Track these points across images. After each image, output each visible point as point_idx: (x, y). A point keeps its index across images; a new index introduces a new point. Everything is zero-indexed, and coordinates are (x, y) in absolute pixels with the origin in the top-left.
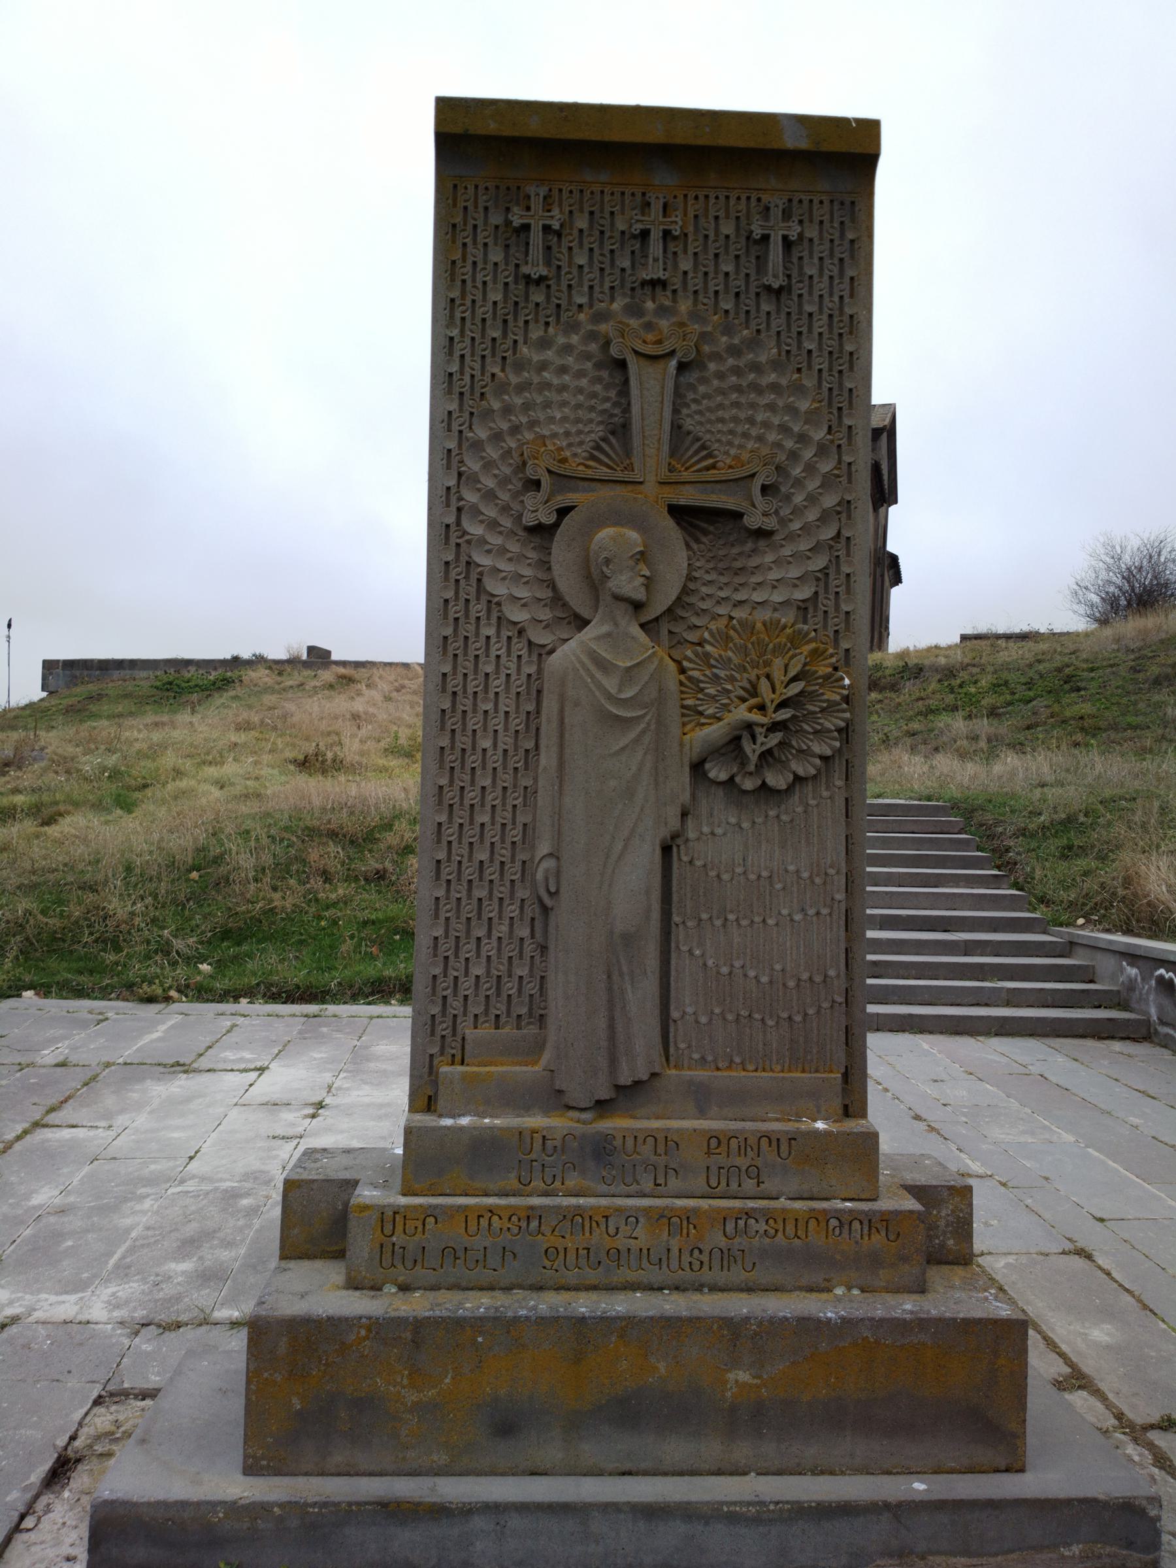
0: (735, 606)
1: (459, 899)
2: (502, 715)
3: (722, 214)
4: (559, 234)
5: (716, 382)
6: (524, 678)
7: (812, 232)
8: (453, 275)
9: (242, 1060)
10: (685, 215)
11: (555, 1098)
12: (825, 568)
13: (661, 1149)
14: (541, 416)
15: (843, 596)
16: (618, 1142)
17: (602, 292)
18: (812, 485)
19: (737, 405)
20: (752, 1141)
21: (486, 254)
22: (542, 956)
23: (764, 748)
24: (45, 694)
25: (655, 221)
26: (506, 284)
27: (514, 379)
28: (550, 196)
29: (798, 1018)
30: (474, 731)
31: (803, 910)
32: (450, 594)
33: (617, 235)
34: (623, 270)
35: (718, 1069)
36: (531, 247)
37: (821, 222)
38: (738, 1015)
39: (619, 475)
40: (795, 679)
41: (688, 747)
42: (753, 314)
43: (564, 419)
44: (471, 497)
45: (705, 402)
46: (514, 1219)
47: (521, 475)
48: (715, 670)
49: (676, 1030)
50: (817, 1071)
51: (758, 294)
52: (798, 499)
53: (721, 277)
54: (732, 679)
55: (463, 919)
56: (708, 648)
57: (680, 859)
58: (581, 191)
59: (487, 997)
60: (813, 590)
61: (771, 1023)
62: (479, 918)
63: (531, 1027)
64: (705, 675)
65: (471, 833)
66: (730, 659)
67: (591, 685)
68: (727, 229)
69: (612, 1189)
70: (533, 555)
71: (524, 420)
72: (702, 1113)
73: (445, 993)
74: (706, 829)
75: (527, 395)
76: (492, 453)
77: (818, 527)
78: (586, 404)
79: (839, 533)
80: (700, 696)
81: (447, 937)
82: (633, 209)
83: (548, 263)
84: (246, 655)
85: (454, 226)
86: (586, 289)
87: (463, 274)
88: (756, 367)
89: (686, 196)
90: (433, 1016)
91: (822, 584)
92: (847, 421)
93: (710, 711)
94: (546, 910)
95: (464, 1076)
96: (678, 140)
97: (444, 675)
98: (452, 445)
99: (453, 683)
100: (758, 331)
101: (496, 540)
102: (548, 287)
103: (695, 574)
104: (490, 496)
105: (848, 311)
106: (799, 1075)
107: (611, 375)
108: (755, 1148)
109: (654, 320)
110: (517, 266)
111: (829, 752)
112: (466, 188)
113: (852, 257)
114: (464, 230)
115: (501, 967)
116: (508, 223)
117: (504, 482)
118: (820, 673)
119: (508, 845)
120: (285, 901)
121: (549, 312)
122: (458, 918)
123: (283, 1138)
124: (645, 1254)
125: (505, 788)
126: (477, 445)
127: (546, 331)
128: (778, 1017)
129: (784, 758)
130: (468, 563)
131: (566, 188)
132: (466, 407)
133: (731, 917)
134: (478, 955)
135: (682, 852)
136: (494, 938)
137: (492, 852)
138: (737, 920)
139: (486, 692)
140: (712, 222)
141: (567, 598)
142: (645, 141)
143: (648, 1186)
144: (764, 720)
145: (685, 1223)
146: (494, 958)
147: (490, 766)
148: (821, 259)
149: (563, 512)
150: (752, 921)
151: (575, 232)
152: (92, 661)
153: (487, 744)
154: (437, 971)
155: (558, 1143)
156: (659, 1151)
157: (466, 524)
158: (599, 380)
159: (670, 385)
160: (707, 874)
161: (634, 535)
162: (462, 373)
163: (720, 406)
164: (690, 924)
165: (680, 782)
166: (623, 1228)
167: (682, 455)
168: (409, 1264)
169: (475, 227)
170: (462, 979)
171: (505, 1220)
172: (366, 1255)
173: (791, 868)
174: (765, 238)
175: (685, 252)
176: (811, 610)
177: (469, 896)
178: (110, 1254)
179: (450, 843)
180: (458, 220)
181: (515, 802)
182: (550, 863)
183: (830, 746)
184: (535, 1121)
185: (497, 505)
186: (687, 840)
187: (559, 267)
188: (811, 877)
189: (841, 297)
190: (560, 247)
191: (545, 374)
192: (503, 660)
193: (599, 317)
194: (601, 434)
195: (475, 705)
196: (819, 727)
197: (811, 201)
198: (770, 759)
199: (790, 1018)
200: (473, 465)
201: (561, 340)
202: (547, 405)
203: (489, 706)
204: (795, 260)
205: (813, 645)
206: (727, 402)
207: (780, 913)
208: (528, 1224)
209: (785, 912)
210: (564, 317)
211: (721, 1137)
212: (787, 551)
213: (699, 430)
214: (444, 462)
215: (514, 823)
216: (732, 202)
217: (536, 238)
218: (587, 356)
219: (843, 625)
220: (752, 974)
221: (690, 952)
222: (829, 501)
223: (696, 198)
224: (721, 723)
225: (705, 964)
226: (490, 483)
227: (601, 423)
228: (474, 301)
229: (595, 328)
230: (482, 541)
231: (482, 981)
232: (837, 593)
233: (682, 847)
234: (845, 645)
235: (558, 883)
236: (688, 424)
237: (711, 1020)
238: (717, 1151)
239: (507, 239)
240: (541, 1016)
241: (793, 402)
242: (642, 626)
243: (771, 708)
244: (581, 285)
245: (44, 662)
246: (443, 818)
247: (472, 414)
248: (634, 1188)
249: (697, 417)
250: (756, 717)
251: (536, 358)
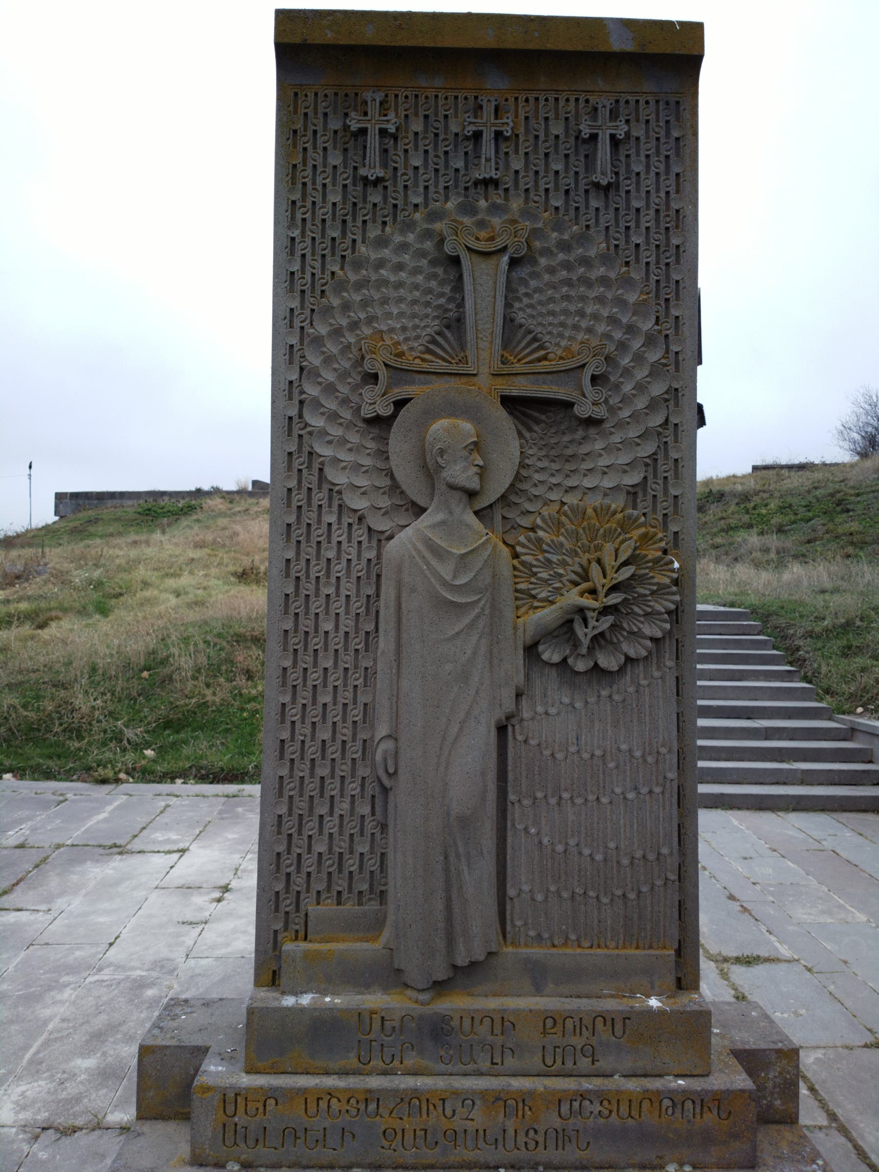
0: (566, 491)
1: (302, 778)
2: (343, 599)
3: (551, 115)
4: (395, 138)
5: (547, 277)
6: (364, 562)
7: (638, 131)
8: (293, 178)
9: (168, 841)
10: (516, 117)
11: (391, 976)
13: (498, 1030)
14: (379, 312)
15: (671, 481)
16: (455, 1023)
17: (436, 192)
18: (641, 374)
19: (567, 298)
20: (587, 1021)
21: (325, 158)
22: (382, 833)
23: (596, 632)
24: (57, 518)
25: (487, 123)
26: (345, 186)
27: (353, 277)
28: (387, 102)
29: (632, 896)
30: (317, 614)
31: (636, 788)
32: (292, 484)
33: (451, 138)
34: (457, 170)
35: (554, 946)
36: (368, 150)
37: (647, 121)
38: (573, 893)
39: (454, 368)
40: (625, 564)
41: (522, 629)
42: (582, 210)
43: (401, 314)
44: (312, 391)
45: (536, 296)
46: (353, 1101)
47: (360, 369)
48: (547, 555)
49: (513, 908)
50: (651, 947)
51: (587, 191)
52: (627, 388)
53: (551, 175)
54: (564, 564)
55: (306, 797)
56: (541, 533)
57: (515, 738)
58: (416, 96)
59: (330, 873)
60: (642, 475)
61: (605, 900)
62: (322, 796)
63: (373, 903)
64: (537, 560)
65: (313, 713)
66: (562, 545)
67: (428, 573)
68: (557, 129)
69: (450, 1068)
70: (371, 445)
71: (362, 316)
72: (538, 990)
73: (288, 870)
74: (540, 709)
75: (366, 292)
76: (332, 348)
77: (647, 414)
78: (422, 300)
79: (667, 421)
80: (533, 580)
81: (290, 815)
82: (467, 112)
83: (384, 165)
84: (206, 487)
85: (295, 132)
86: (421, 189)
87: (304, 178)
88: (585, 261)
89: (516, 99)
90: (277, 893)
91: (651, 469)
92: (674, 312)
93: (543, 595)
94: (385, 790)
95: (306, 954)
96: (509, 45)
97: (288, 561)
98: (294, 340)
99: (298, 568)
100: (588, 227)
101: (336, 431)
102: (385, 188)
103: (527, 461)
104: (330, 389)
105: (674, 206)
106: (632, 952)
107: (445, 271)
108: (590, 1027)
109: (487, 218)
110: (355, 168)
111: (659, 634)
112: (306, 96)
113: (678, 154)
114: (305, 135)
115: (342, 844)
116: (346, 128)
117: (343, 375)
118: (650, 557)
119: (349, 724)
120: (214, 697)
121: (386, 212)
122: (301, 796)
123: (191, 923)
124: (480, 1135)
125: (346, 669)
126: (318, 341)
127: (383, 231)
128: (613, 894)
129: (615, 640)
130: (310, 453)
131: (402, 93)
132: (307, 304)
133: (566, 795)
134: (321, 833)
135: (517, 734)
136: (336, 815)
137: (334, 732)
138: (571, 798)
139: (328, 577)
140: (543, 123)
141: (404, 487)
142: (477, 46)
143: (484, 1064)
145: (520, 1105)
146: (336, 835)
147: (332, 647)
148: (647, 156)
149: (400, 404)
150: (586, 800)
151: (411, 136)
152: (91, 493)
153: (328, 626)
154: (281, 848)
155: (397, 1024)
156: (495, 1032)
157: (307, 417)
158: (435, 276)
159: (502, 279)
160: (541, 753)
161: (467, 426)
162: (303, 272)
163: (551, 300)
164: (526, 802)
166: (459, 1110)
167: (515, 347)
169: (315, 132)
170: (305, 856)
171: (344, 1102)
172: (210, 1134)
173: (624, 747)
174: (594, 137)
175: (517, 152)
176: (640, 495)
177: (312, 775)
178: (26, 1048)
179: (293, 723)
180: (299, 126)
181: (356, 683)
182: (388, 745)
183: (660, 628)
184: (374, 1000)
185: (337, 397)
186: (522, 720)
187: (395, 169)
188: (643, 756)
189: (668, 193)
190: (396, 149)
191: (383, 272)
192: (345, 545)
193: (434, 216)
194: (436, 328)
195: (317, 589)
196: (649, 610)
197: (637, 101)
198: (602, 642)
199: (624, 895)
200: (314, 360)
201: (398, 239)
202: (385, 301)
203: (331, 590)
204: (623, 158)
205: (643, 530)
206: (557, 296)
207: (613, 792)
208: (366, 1106)
209: (618, 790)
211: (556, 1018)
212: (617, 438)
213: (531, 323)
214: (287, 357)
215: (355, 703)
216: (562, 103)
217: (373, 141)
218: (423, 254)
219: (671, 509)
220: (586, 852)
221: (526, 829)
222: (658, 389)
223: (527, 100)
224: (553, 607)
225: (540, 843)
226: (329, 376)
227: (437, 317)
228: (314, 203)
229: (430, 227)
230: (323, 433)
231: (325, 858)
232: (666, 478)
233: (517, 727)
234: (673, 528)
235: (396, 764)
236: (520, 317)
237: (546, 897)
238: (553, 1031)
239: (345, 143)
240: (382, 892)
241: (622, 294)
242: (476, 513)
243: (602, 592)
244: (416, 185)
245: (57, 494)
246: (287, 699)
247: (313, 311)
248: (471, 1067)
249: (529, 311)
250: (587, 601)
251: (373, 256)
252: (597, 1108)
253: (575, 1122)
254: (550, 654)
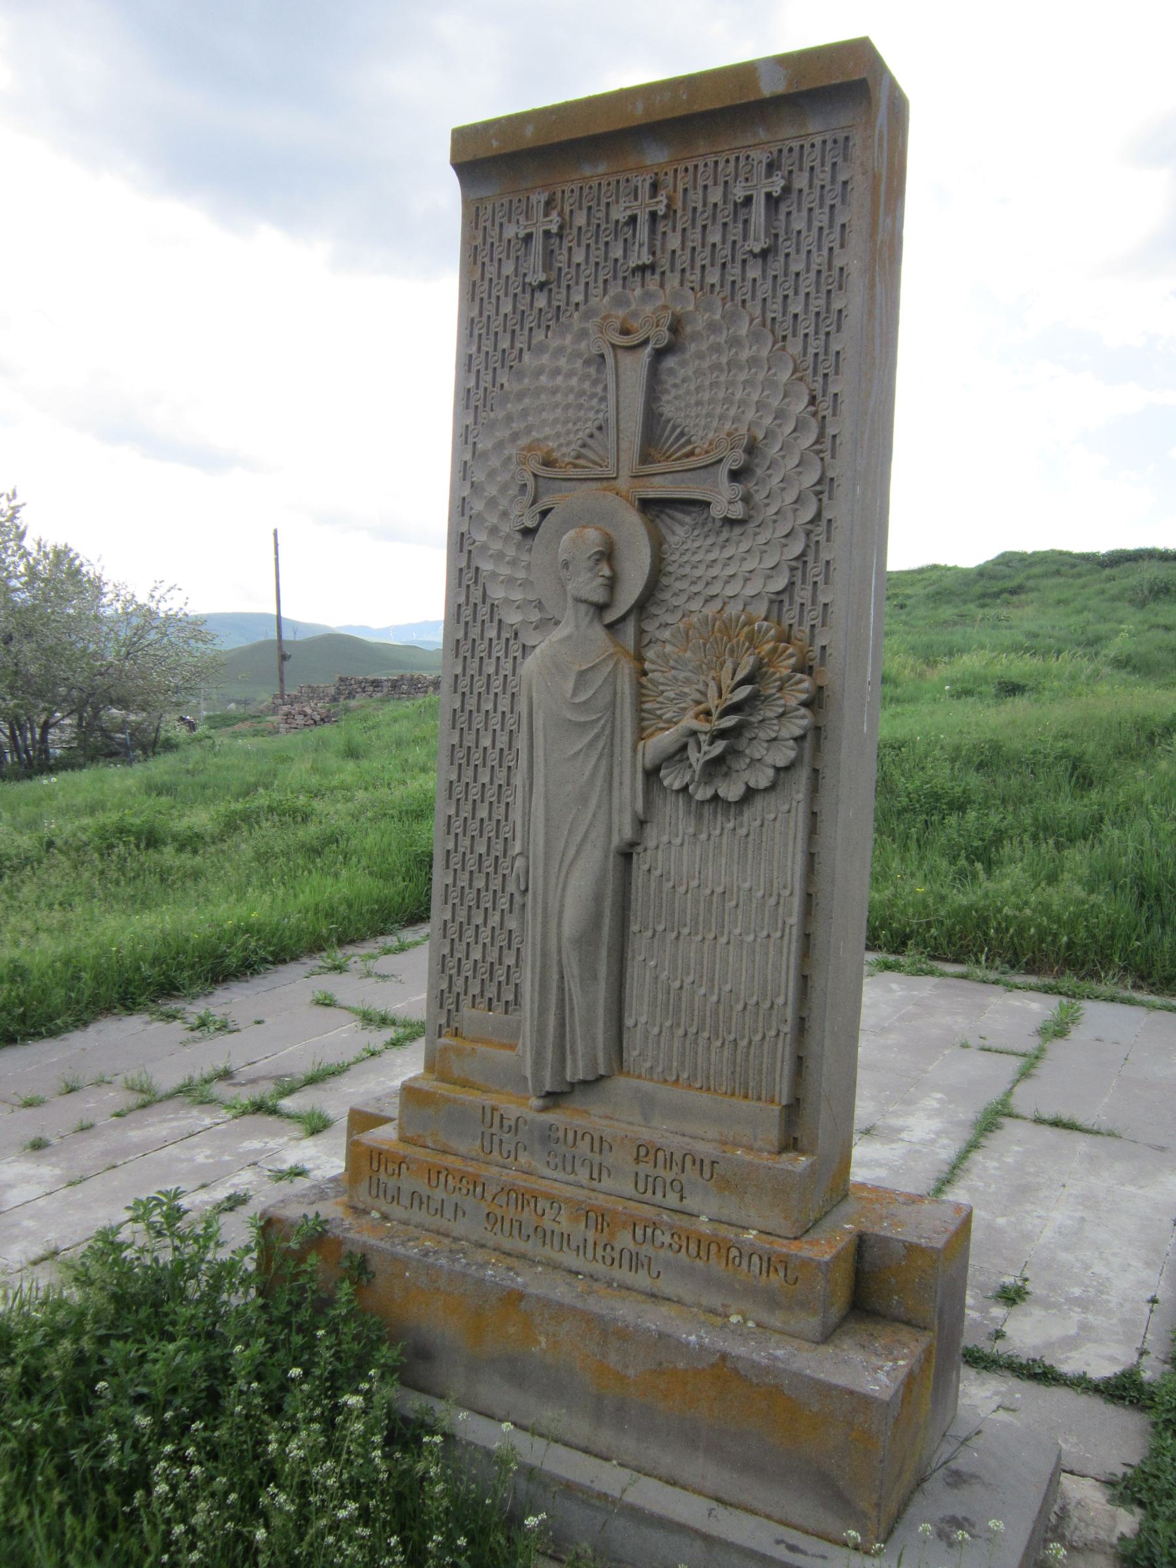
3: (710, 182)
15: (821, 586)
20: (677, 1157)
69: (555, 1175)
80: (660, 699)
91: (799, 573)
147: (489, 764)
149: (544, 514)
155: (513, 1123)
165: (629, 791)
204: (782, 217)
216: (721, 166)
223: (686, 170)
248: (572, 1178)
250: (696, 725)
252: (667, 1239)
253: (647, 1250)
254: (672, 779)
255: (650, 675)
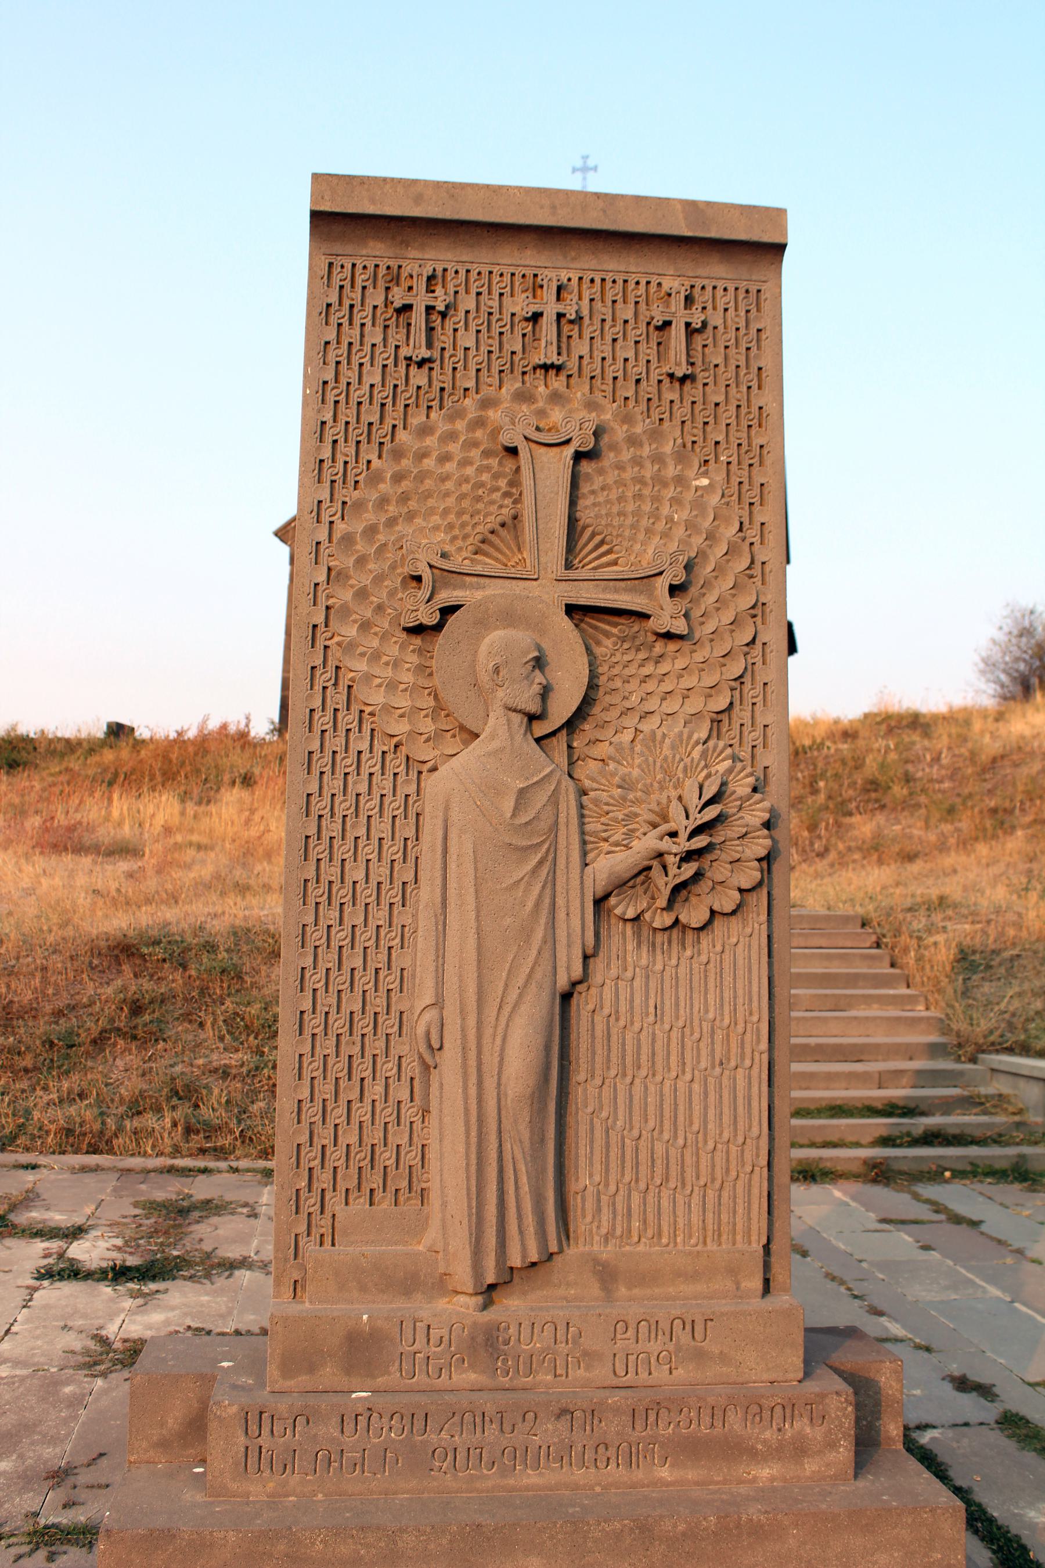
7: (716, 319)
10: (580, 299)
12: (741, 677)
20: (665, 1325)
23: (678, 881)
36: (413, 328)
83: (429, 345)
91: (737, 693)
108: (668, 1333)
112: (342, 267)
144: (675, 849)
149: (447, 611)
168: (278, 1467)
210: (448, 403)
217: (418, 317)
222: (745, 601)
242: (538, 740)
250: (666, 844)
254: (624, 907)
255: (592, 794)
